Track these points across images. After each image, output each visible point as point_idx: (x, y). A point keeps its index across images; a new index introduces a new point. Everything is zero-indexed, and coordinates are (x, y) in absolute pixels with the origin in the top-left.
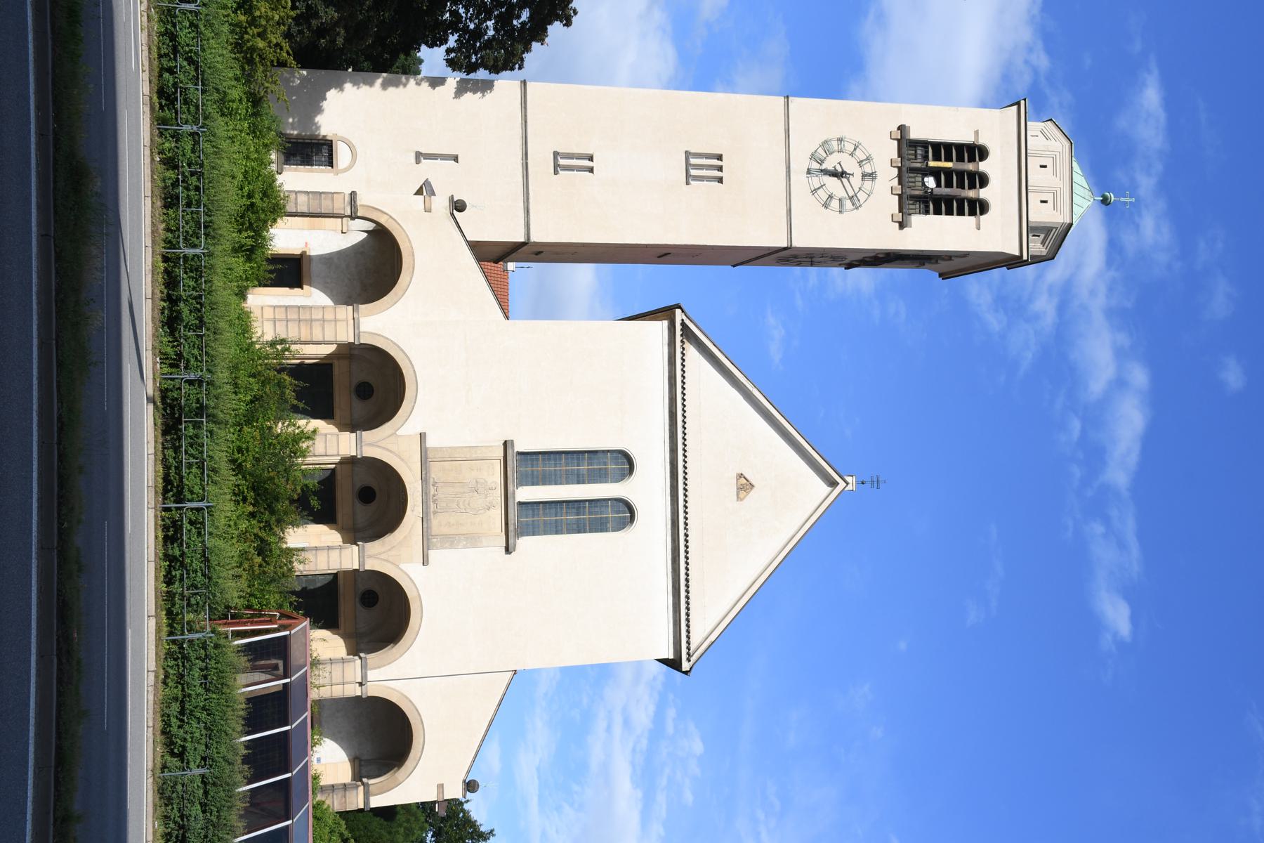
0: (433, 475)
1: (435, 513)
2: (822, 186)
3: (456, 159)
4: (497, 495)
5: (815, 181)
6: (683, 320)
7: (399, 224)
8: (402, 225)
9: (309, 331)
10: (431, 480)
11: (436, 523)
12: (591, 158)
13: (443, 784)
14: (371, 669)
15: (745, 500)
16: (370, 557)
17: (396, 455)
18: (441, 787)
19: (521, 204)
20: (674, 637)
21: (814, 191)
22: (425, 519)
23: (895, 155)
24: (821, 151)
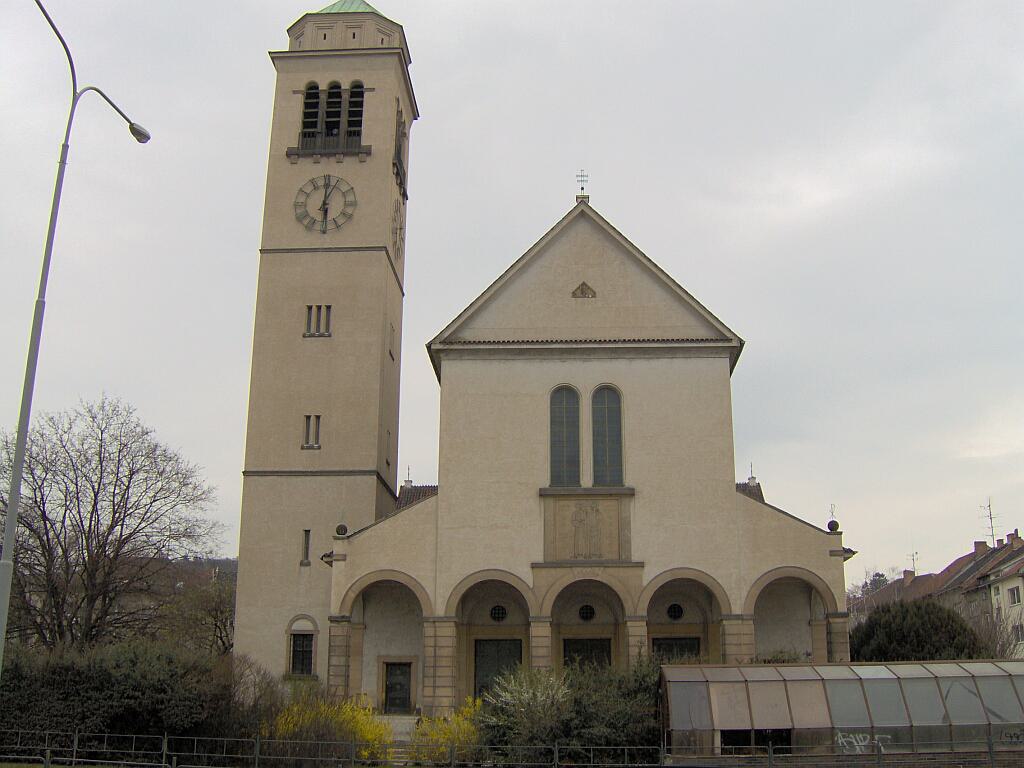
1: (601, 556)
4: (587, 504)
5: (331, 226)
11: (609, 554)
12: (308, 417)
13: (831, 552)
15: (596, 291)
24: (306, 222)
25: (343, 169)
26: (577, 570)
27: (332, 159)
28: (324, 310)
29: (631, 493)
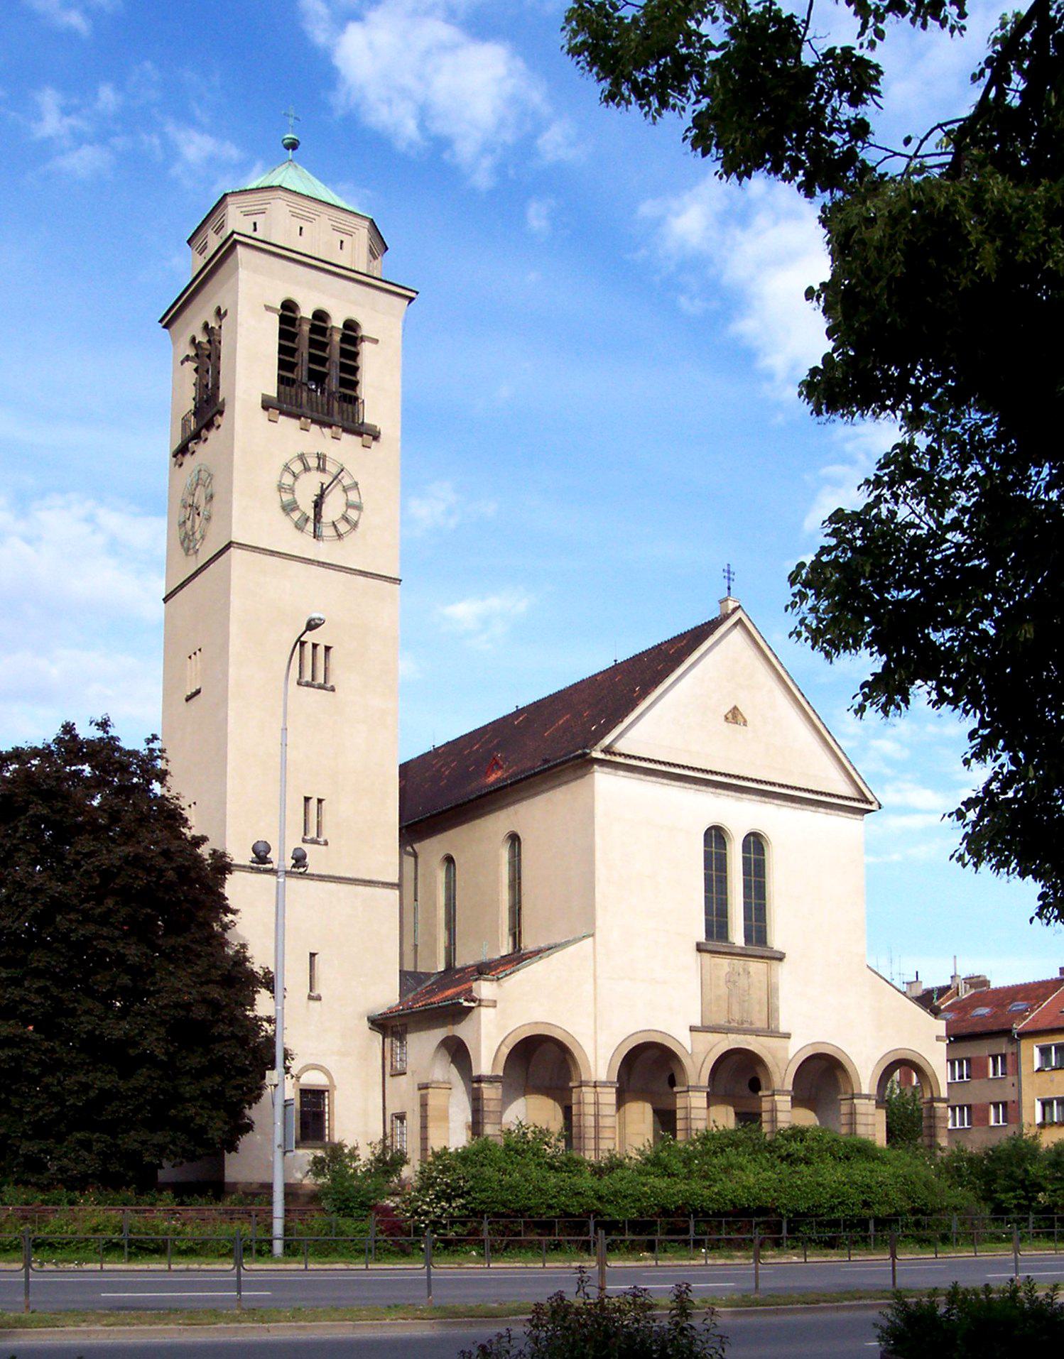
1: (751, 1023)
2: (334, 524)
4: (738, 963)
5: (327, 531)
6: (602, 751)
7: (509, 1035)
8: (510, 1031)
9: (607, 1129)
10: (727, 1024)
11: (760, 1023)
12: (307, 799)
14: (861, 1090)
16: (783, 1084)
17: (707, 1055)
21: (340, 536)
22: (757, 1033)
26: (732, 1036)
27: (326, 431)
28: (321, 650)
29: (780, 958)
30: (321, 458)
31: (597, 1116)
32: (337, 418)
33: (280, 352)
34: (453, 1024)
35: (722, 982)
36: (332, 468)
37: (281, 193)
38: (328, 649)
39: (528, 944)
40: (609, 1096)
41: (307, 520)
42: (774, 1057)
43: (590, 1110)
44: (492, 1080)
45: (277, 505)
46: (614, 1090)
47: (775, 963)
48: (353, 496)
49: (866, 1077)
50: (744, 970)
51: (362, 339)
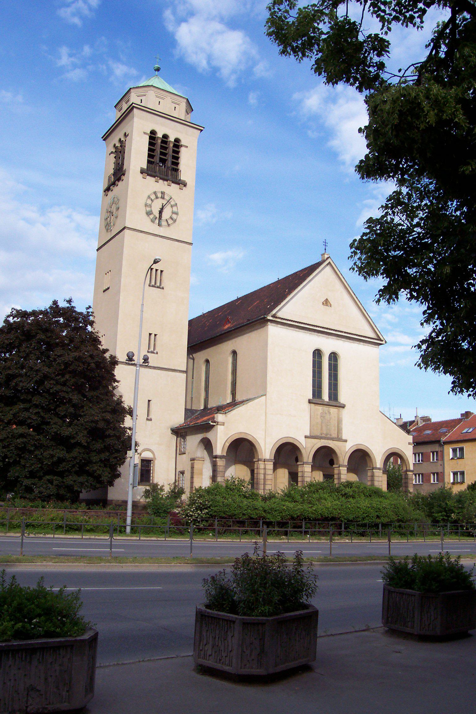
0: (319, 434)
1: (331, 435)
3: (149, 401)
4: (326, 408)
5: (164, 223)
6: (272, 316)
11: (334, 435)
12: (150, 334)
18: (409, 444)
19: (170, 373)
20: (371, 344)
22: (333, 439)
23: (153, 179)
25: (172, 190)
27: (166, 182)
28: (159, 272)
29: (343, 407)
30: (163, 193)
31: (265, 474)
32: (170, 177)
33: (149, 151)
34: (206, 432)
35: (319, 417)
36: (167, 198)
37: (152, 88)
38: (162, 271)
39: (239, 398)
40: (270, 466)
41: (156, 218)
42: (340, 450)
43: (262, 471)
44: (221, 457)
45: (144, 212)
46: (272, 463)
47: (341, 409)
48: (175, 209)
49: (378, 460)
50: (328, 412)
51: (181, 146)
